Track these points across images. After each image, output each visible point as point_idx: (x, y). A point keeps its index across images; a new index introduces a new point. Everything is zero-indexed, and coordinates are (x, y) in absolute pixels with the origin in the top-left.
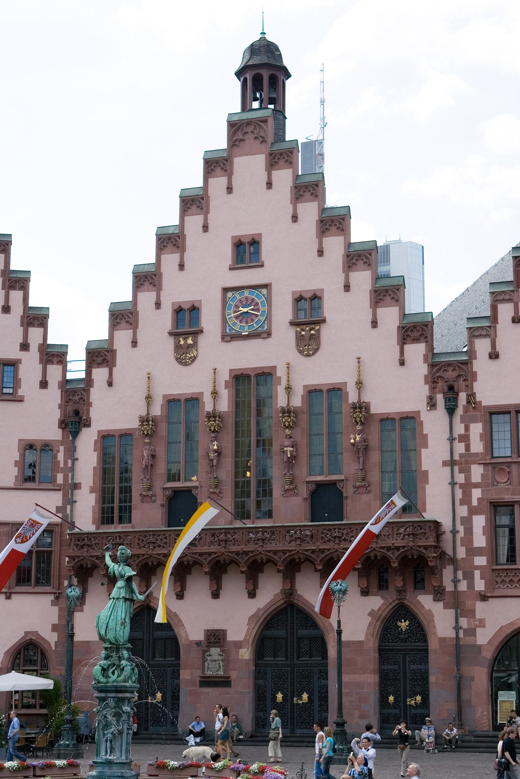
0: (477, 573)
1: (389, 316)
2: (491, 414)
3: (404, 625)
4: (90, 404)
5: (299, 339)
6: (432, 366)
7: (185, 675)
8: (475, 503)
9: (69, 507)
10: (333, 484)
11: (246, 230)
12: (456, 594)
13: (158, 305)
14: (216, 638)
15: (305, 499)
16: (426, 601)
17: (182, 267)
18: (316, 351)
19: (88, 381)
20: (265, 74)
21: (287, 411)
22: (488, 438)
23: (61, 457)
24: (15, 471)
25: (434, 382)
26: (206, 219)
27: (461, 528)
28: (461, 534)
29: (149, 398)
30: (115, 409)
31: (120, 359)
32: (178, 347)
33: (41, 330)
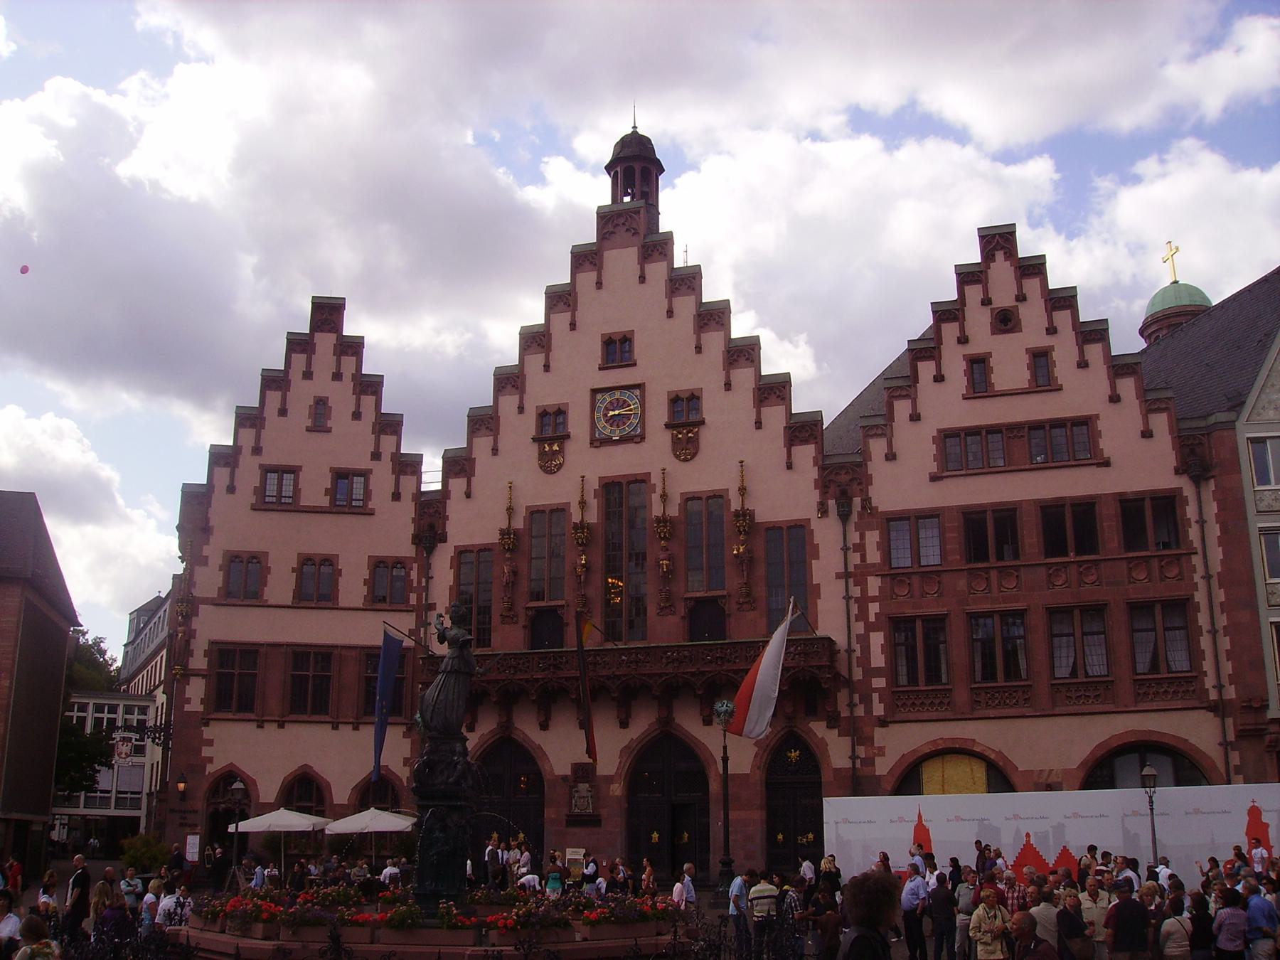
0: (875, 696)
2: (889, 520)
3: (794, 755)
4: (446, 518)
5: (675, 442)
6: (822, 469)
7: (549, 813)
8: (872, 618)
10: (714, 600)
12: (852, 719)
13: (521, 409)
14: (583, 772)
15: (683, 618)
16: (819, 728)
17: (547, 367)
18: (694, 455)
19: (444, 493)
20: (637, 167)
21: (663, 520)
22: (885, 547)
23: (414, 575)
25: (826, 487)
26: (573, 316)
27: (857, 647)
28: (858, 653)
29: (510, 510)
30: (473, 524)
31: (478, 469)
32: (542, 454)
33: (395, 438)
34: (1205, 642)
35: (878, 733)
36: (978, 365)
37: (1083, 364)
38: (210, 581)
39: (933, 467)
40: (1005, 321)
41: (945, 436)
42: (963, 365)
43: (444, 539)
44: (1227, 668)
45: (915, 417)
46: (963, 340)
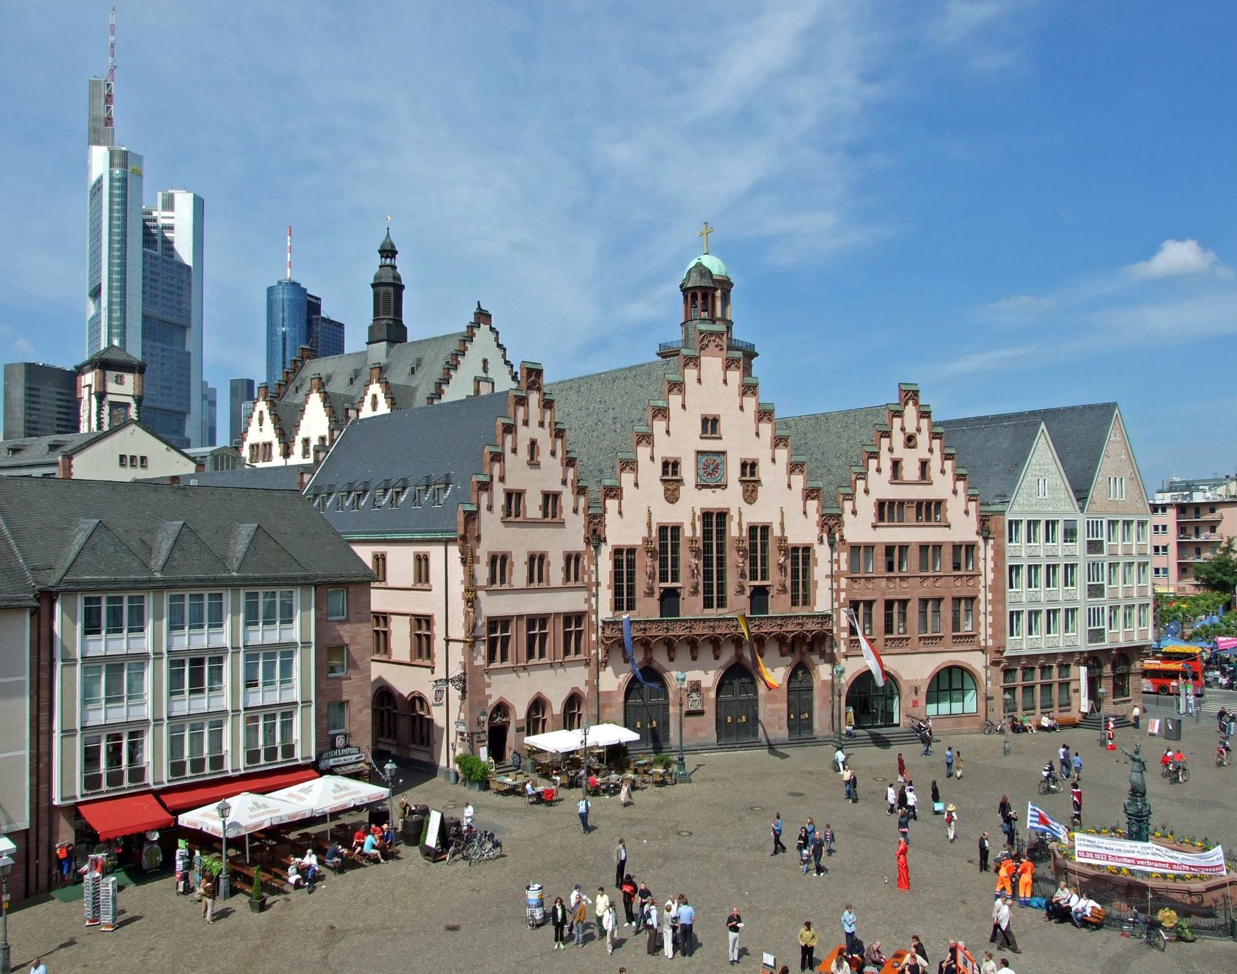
1: (798, 481)
7: (673, 710)
9: (593, 599)
11: (711, 411)
13: (652, 458)
24: (562, 574)
32: (666, 490)
34: (982, 618)
35: (843, 661)
36: (896, 464)
37: (943, 472)
38: (482, 572)
39: (873, 520)
40: (910, 441)
41: (881, 504)
42: (890, 464)
43: (605, 540)
44: (990, 631)
45: (867, 491)
46: (891, 450)
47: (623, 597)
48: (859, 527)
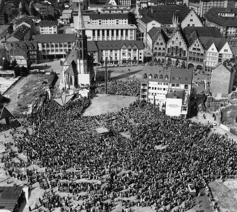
38: (154, 49)
40: (197, 42)
47: (168, 52)
48: (191, 49)
